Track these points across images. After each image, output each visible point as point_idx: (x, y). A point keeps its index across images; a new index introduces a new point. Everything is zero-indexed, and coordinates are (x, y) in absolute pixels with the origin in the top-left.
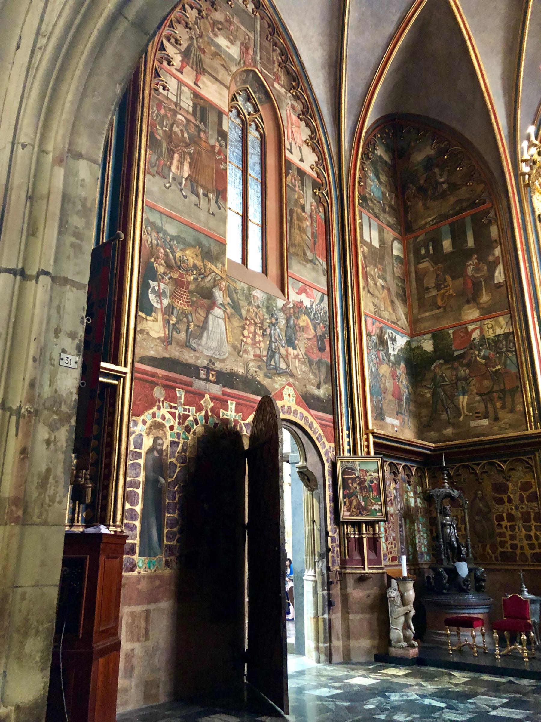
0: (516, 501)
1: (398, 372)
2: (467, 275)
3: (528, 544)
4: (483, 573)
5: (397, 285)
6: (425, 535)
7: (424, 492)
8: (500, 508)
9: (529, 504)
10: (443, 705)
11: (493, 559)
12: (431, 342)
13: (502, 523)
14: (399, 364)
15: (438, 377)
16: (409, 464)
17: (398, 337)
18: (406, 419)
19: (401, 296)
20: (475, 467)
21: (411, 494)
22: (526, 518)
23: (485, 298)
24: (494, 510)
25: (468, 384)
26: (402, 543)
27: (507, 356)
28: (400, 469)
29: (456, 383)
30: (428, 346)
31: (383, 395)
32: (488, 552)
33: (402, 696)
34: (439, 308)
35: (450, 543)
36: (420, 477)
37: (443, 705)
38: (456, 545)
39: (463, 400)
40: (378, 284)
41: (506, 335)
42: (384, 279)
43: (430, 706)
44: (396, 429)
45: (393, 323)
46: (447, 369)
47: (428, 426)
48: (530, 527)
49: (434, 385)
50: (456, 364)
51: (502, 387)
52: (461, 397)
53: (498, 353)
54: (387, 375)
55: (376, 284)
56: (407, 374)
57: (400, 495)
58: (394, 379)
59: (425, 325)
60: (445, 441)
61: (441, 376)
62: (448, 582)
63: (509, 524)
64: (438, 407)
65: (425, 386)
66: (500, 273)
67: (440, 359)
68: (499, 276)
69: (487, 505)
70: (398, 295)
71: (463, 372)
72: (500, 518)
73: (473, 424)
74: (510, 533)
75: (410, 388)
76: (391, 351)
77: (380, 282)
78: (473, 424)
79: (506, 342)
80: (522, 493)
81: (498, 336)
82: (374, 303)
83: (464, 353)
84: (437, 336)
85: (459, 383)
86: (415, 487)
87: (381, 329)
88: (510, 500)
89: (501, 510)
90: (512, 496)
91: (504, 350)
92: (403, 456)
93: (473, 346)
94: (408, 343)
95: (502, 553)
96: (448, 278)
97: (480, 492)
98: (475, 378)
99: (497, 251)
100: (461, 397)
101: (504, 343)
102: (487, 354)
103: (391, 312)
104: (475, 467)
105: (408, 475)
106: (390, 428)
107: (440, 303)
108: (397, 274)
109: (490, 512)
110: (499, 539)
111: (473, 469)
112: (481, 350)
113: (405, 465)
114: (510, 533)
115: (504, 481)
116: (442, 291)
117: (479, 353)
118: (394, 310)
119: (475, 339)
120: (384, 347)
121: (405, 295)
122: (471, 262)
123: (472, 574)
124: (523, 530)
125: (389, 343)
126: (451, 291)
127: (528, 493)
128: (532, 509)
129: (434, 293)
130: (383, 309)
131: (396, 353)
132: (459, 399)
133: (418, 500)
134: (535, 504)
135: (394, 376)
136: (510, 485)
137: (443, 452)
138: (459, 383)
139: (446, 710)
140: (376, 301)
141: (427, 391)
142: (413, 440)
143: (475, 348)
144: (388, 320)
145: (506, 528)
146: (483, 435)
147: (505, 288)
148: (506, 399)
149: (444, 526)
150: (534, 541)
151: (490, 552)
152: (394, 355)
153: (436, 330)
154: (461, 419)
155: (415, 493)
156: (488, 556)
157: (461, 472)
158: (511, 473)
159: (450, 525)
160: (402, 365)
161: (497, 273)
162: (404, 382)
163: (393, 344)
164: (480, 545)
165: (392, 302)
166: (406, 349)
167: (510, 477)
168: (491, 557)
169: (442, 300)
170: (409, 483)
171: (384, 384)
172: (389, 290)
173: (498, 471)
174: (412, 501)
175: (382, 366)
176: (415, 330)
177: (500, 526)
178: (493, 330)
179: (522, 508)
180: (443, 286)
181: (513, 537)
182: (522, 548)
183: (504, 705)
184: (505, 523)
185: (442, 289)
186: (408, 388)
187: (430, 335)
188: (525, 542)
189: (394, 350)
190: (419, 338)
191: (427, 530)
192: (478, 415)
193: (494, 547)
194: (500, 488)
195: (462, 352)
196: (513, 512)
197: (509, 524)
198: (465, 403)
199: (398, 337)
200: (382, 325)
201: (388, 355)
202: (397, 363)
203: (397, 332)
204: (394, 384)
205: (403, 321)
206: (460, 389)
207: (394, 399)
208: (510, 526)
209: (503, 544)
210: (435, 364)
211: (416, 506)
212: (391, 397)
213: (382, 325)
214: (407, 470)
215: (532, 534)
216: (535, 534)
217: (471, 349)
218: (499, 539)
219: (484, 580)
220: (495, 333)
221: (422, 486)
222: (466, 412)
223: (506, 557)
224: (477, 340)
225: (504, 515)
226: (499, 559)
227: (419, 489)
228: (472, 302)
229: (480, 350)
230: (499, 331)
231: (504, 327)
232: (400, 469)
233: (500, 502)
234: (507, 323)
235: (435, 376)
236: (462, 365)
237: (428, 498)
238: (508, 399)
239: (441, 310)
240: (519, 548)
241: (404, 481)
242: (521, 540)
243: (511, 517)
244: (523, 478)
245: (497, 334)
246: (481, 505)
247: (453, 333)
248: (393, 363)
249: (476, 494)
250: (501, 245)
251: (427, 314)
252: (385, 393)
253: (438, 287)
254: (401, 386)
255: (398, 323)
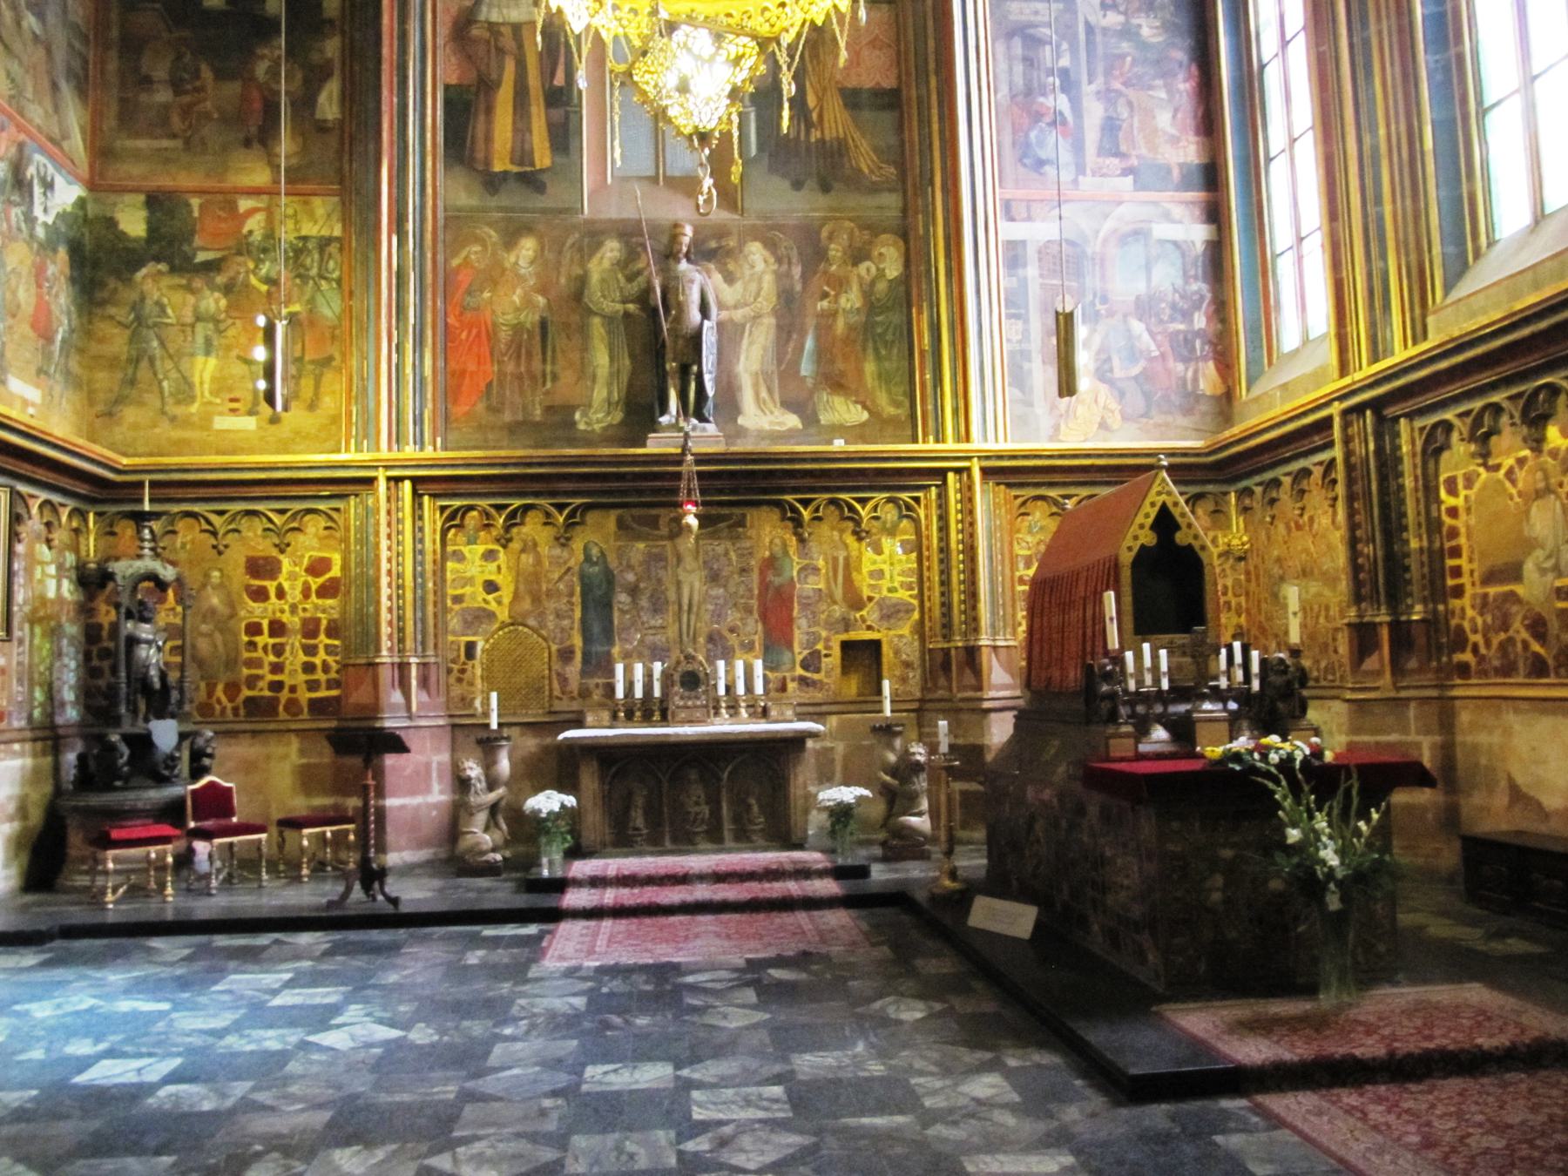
0: (294, 594)
1: (51, 270)
2: (253, 79)
3: (307, 682)
4: (208, 741)
5: (70, 45)
6: (73, 665)
7: (80, 568)
8: (257, 607)
9: (320, 602)
10: (165, 1006)
11: (229, 712)
12: (143, 214)
13: (257, 639)
14: (55, 251)
15: (149, 302)
16: (56, 498)
17: (60, 181)
18: (58, 389)
19: (76, 76)
20: (214, 518)
21: (52, 570)
22: (310, 628)
23: (285, 146)
24: (243, 613)
25: (220, 332)
26: (20, 681)
27: (318, 287)
28: (35, 511)
29: (193, 326)
30: (133, 223)
31: (10, 321)
32: (219, 701)
33: (59, 1006)
34: (174, 136)
35: (145, 682)
36: (77, 531)
37: (165, 1006)
38: (157, 685)
39: (205, 369)
40: (25, 24)
41: (324, 243)
42: (41, 16)
43: (135, 1014)
44: (31, 410)
45: (51, 140)
46: (171, 287)
47: (110, 414)
48: (315, 647)
49: (138, 318)
50: (198, 283)
51: (298, 354)
52: (200, 359)
53: (299, 276)
54: (25, 270)
55: (18, 24)
56: (73, 280)
57: (25, 569)
58: (39, 286)
59: (133, 171)
60: (151, 455)
61: (158, 303)
62: (129, 763)
63: (272, 641)
64: (139, 375)
65: (111, 318)
66: (330, 98)
67: (158, 260)
68: (329, 104)
69: (232, 605)
70: (70, 74)
71: (213, 302)
72: (254, 629)
73: (223, 423)
74: (272, 658)
75: (74, 316)
76: (38, 211)
77: (30, 21)
78: (223, 423)
79: (322, 259)
80: (310, 579)
81: (305, 239)
82: (8, 74)
83: (223, 259)
84: (157, 202)
85: (200, 327)
86: (61, 552)
87: (21, 147)
88: (281, 594)
89: (258, 612)
90: (286, 585)
91: (314, 272)
92: (50, 477)
93: (243, 247)
94: (81, 203)
95: (249, 700)
96: (207, 73)
97: (216, 574)
98: (238, 322)
99: (332, 47)
100: (200, 359)
101: (316, 256)
102: (273, 275)
103: (51, 111)
104: (214, 518)
105: (48, 525)
106: (18, 404)
107: (176, 122)
108: (72, 17)
109: (233, 615)
110: (246, 672)
111: (208, 522)
112: (263, 261)
113: (47, 502)
114: (272, 658)
115: (275, 552)
116: (186, 99)
117: (256, 267)
118: (57, 109)
119: (251, 232)
120: (22, 196)
121: (86, 76)
122: (266, 51)
123: (186, 744)
124: (301, 652)
125: (37, 190)
126: (208, 104)
127: (321, 580)
128: (324, 611)
129: (163, 96)
130: (29, 95)
131: (50, 221)
132: (192, 364)
133: (66, 584)
134: (330, 602)
135: (39, 274)
136: (286, 563)
137: (147, 478)
138: (200, 327)
139: (174, 1015)
140: (15, 67)
141: (116, 331)
142: (81, 441)
143: (249, 252)
144: (39, 128)
145: (265, 648)
146: (242, 451)
147: (337, 132)
148: (303, 382)
149: (133, 641)
150: (320, 676)
151: (224, 699)
152: (45, 224)
153: (159, 190)
154: (194, 408)
155: (60, 567)
156: (218, 707)
157: (180, 525)
158: (290, 537)
159: (149, 642)
160: (62, 253)
161: (323, 98)
162: (62, 299)
163: (45, 194)
164: (203, 685)
165: (55, 87)
166: (76, 218)
167: (288, 545)
168: (224, 710)
169: (183, 119)
170: (48, 542)
171: (14, 293)
172: (49, 51)
173: (266, 530)
174: (51, 585)
175: (14, 245)
176: (102, 175)
177: (252, 645)
178: (296, 222)
179: (305, 610)
180: (189, 87)
181: (277, 668)
182: (293, 689)
183: (289, 985)
184: (264, 639)
185: (186, 92)
186: (69, 313)
187: (142, 198)
188: (302, 677)
189: (45, 210)
190: (113, 198)
191: (77, 652)
192: (235, 405)
193: (232, 689)
194: (261, 568)
195: (218, 255)
196: (286, 618)
197: (272, 641)
198: (207, 377)
199: (60, 181)
200: (22, 137)
201: (30, 219)
202: (49, 246)
203: (59, 166)
204: (40, 297)
205: (77, 144)
206: (200, 340)
207: (31, 334)
208: (274, 646)
209: (252, 682)
210: (144, 271)
211: (59, 597)
212: (25, 329)
213: (22, 137)
214: (47, 511)
215: (317, 661)
216: (324, 663)
217: (239, 253)
218: (246, 672)
219: (210, 756)
220: (298, 230)
221: (77, 551)
222: (207, 394)
223: (260, 709)
224: (257, 237)
225: (265, 624)
226: (242, 712)
227: (70, 559)
228: (256, 145)
229: (259, 261)
230: (309, 229)
231: (321, 223)
232: (35, 511)
233: (260, 595)
234: (329, 216)
235: (143, 299)
236: (213, 287)
237: (92, 581)
238: (307, 384)
239: (179, 143)
240: (286, 690)
241: (38, 537)
242: (293, 672)
243: (277, 628)
244: (313, 549)
245: (304, 233)
246: (215, 601)
247: (201, 206)
248: (41, 245)
249: (207, 576)
250: (343, 33)
251: (142, 144)
252: (14, 316)
253: (177, 86)
254: (53, 307)
255: (65, 145)
